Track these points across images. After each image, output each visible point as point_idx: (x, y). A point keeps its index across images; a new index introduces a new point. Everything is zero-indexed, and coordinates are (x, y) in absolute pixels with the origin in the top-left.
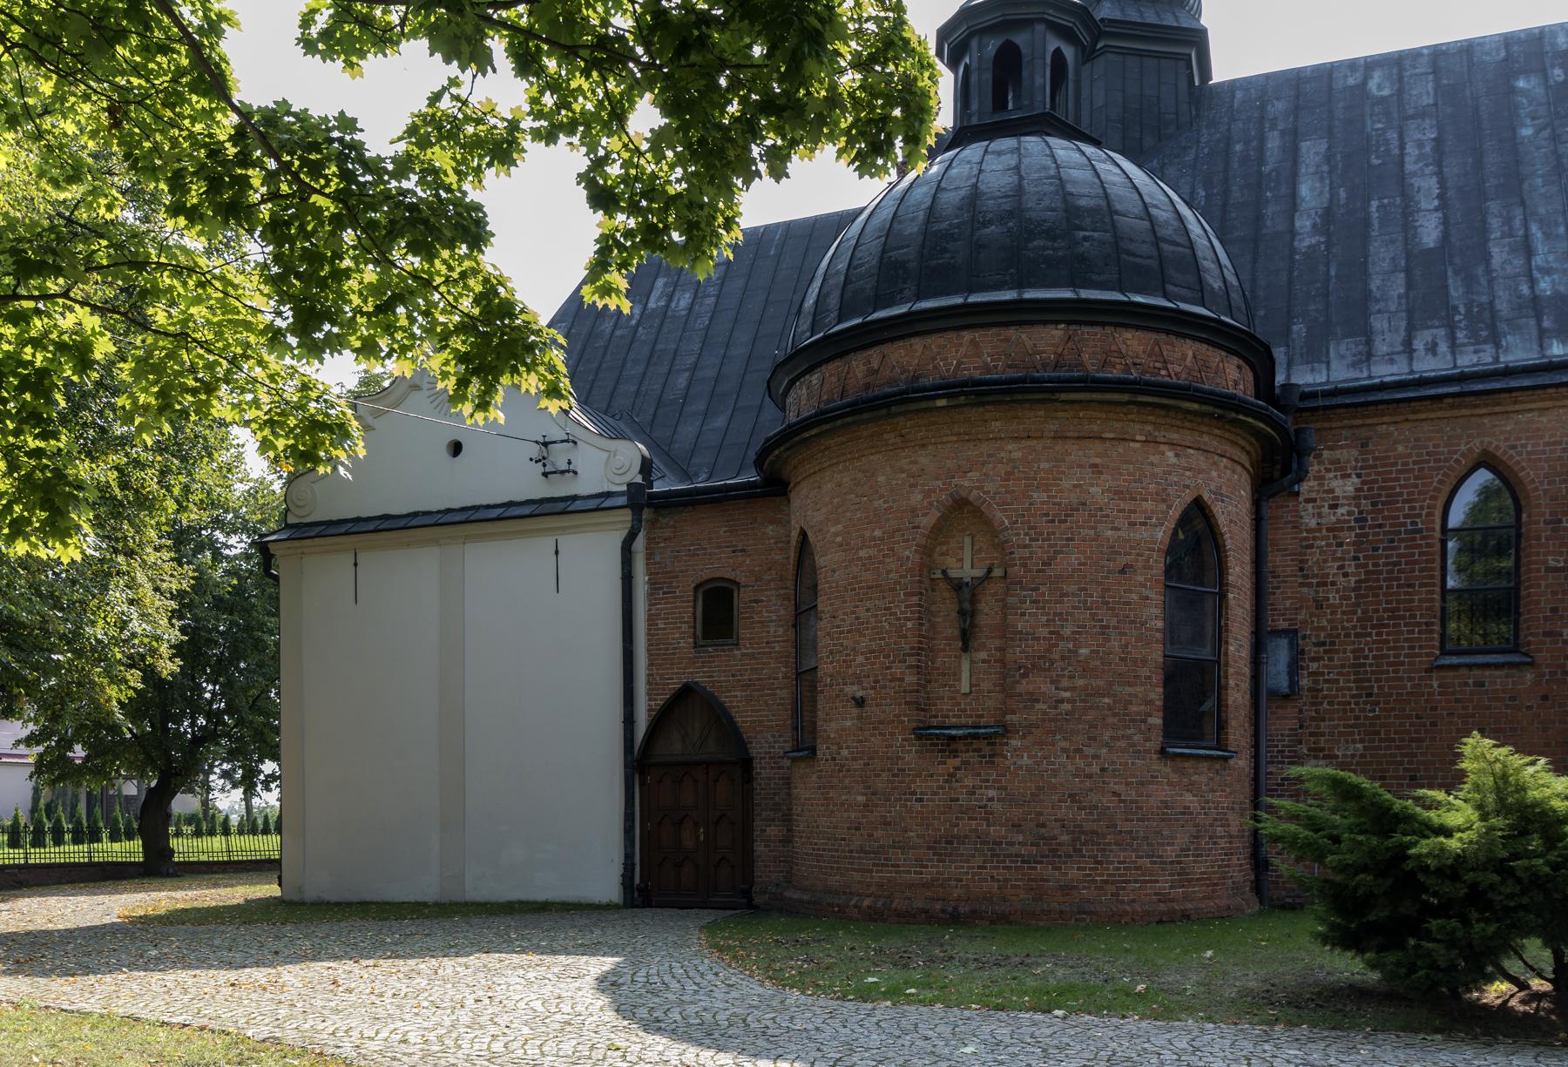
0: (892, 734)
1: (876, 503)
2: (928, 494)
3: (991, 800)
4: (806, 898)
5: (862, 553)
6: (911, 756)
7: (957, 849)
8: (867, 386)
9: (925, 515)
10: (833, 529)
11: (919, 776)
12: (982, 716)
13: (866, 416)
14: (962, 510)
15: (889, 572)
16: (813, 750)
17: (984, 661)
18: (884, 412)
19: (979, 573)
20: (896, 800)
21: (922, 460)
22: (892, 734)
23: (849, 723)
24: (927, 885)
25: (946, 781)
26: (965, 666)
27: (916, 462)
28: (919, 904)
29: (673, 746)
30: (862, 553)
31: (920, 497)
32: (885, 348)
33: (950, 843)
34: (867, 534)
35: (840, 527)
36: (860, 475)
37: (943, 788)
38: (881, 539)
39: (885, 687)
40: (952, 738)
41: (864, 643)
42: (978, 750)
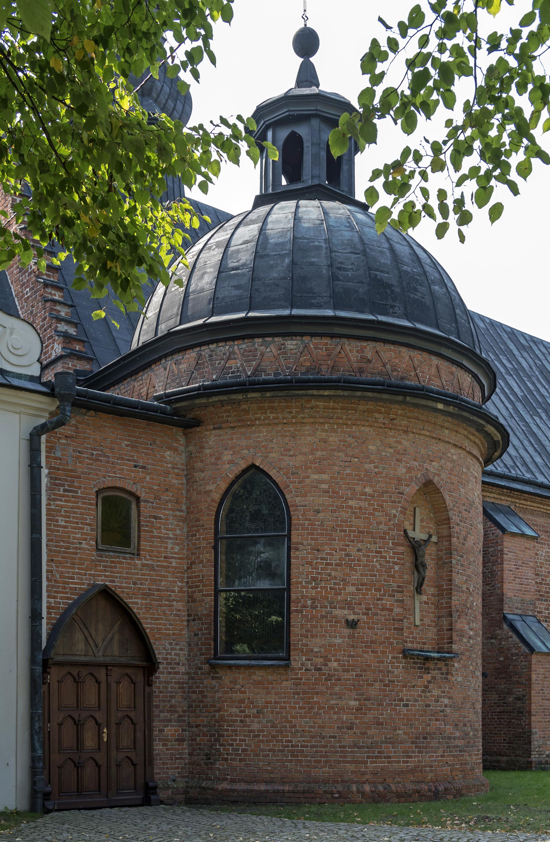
0: (383, 652)
1: (367, 466)
2: (410, 469)
4: (286, 788)
5: (351, 503)
6: (399, 670)
7: (429, 743)
8: (361, 371)
9: (407, 485)
10: (316, 477)
11: (405, 686)
12: (424, 643)
13: (385, 396)
14: (429, 488)
15: (379, 523)
16: (289, 659)
17: (426, 603)
18: (400, 398)
19: (424, 537)
20: (388, 705)
21: (405, 443)
22: (383, 652)
23: (338, 641)
24: (413, 771)
25: (423, 691)
26: (417, 605)
27: (400, 443)
28: (411, 787)
29: (78, 647)
30: (351, 503)
31: (404, 470)
32: (379, 346)
34: (358, 488)
35: (325, 477)
36: (350, 440)
37: (421, 696)
38: (372, 496)
39: (376, 614)
40: (427, 659)
41: (355, 577)
42: (440, 669)
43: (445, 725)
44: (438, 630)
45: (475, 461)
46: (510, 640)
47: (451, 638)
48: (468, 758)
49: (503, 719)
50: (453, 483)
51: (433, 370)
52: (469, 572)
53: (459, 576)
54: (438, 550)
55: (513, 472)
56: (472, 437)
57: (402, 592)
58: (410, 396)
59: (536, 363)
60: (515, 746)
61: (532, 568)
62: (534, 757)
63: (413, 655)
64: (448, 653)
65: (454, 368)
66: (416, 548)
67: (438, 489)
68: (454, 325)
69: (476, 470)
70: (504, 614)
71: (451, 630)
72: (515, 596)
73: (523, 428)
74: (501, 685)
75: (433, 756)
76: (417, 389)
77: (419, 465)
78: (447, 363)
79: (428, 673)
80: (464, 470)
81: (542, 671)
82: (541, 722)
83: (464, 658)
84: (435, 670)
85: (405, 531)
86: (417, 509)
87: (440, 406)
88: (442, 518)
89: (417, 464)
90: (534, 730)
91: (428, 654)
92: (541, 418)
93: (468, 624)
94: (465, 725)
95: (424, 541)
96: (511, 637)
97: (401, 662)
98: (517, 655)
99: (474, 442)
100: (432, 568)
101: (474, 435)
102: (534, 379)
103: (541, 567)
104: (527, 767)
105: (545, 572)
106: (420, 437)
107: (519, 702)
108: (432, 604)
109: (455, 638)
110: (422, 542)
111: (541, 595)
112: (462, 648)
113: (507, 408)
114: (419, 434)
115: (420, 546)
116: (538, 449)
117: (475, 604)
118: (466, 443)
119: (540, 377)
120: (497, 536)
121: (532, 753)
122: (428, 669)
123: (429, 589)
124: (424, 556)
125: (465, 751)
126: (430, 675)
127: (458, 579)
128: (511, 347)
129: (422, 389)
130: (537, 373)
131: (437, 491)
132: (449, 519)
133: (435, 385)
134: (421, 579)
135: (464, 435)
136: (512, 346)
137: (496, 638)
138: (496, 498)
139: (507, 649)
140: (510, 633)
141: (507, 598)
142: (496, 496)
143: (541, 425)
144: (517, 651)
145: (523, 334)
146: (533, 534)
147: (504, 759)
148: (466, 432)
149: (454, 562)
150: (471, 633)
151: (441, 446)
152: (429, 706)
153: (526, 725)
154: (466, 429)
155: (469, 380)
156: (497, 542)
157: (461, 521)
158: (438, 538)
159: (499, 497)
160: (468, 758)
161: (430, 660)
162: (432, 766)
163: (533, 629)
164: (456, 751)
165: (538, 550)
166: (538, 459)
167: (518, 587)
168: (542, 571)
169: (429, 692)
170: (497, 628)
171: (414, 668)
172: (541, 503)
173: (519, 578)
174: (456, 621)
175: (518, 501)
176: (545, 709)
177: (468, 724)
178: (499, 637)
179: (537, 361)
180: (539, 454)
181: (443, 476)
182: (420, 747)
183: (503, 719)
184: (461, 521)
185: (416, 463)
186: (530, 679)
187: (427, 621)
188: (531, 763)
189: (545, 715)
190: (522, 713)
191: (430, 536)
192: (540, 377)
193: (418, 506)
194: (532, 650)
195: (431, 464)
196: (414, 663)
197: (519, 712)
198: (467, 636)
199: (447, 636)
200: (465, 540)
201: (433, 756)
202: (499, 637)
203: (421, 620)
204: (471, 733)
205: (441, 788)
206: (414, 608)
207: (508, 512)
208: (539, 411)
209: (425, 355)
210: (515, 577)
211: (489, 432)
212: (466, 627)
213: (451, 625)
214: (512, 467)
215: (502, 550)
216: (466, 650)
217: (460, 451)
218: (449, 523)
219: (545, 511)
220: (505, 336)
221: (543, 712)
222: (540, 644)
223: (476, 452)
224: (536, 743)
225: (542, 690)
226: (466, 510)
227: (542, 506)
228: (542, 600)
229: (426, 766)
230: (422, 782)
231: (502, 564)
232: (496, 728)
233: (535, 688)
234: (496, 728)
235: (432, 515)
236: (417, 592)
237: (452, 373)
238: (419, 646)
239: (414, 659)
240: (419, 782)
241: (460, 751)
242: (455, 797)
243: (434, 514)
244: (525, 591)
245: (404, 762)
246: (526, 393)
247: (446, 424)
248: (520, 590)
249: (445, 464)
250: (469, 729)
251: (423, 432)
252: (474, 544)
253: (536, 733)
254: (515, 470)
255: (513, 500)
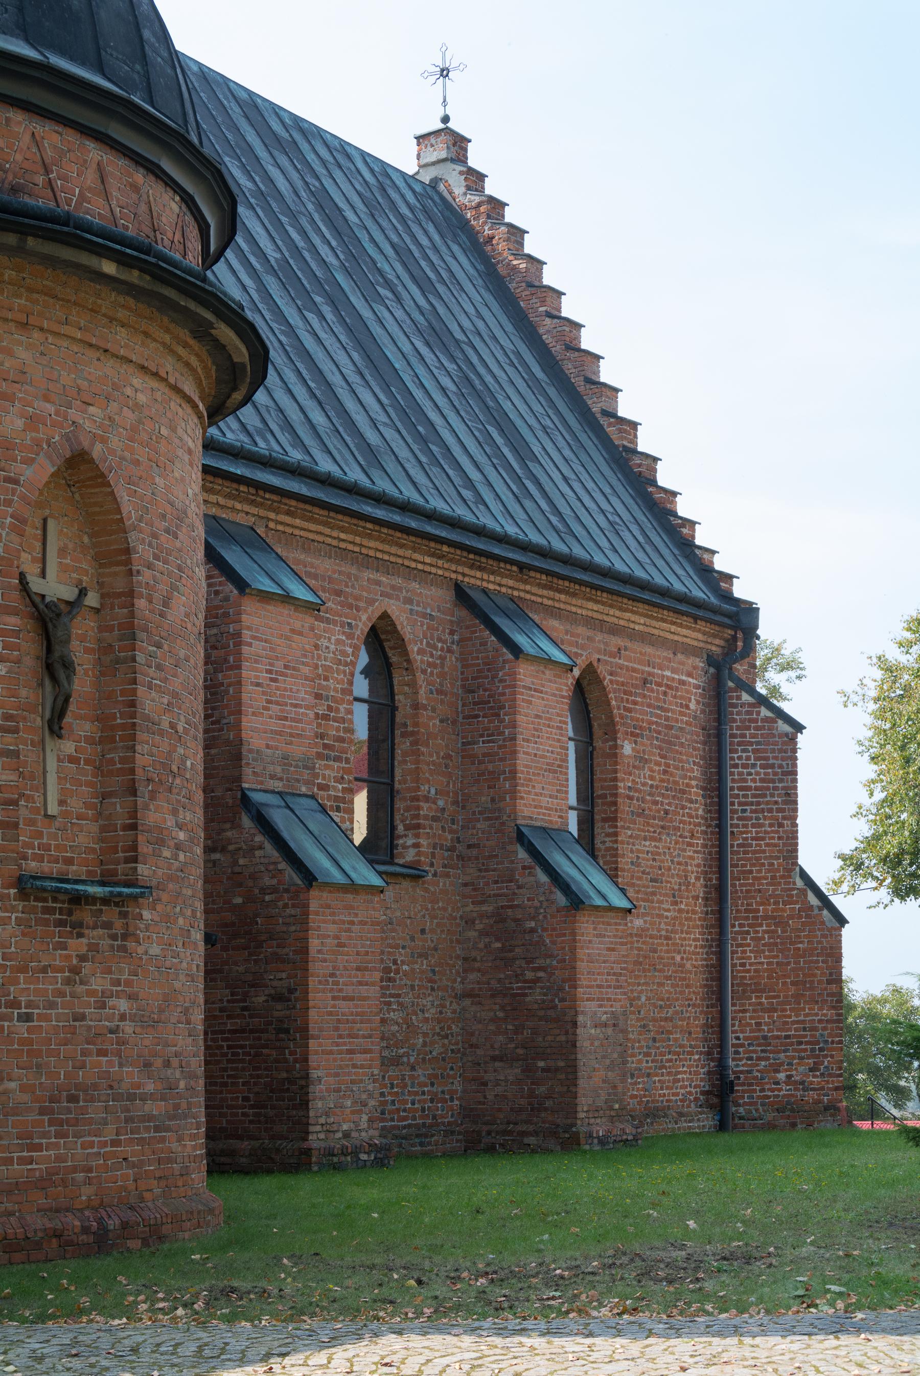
3: (123, 1017)
11: (23, 969)
12: (69, 861)
14: (80, 473)
17: (72, 760)
19: (68, 593)
24: (43, 1183)
25: (68, 982)
26: (52, 764)
28: (38, 1222)
33: (73, 1099)
37: (62, 994)
40: (77, 899)
42: (108, 925)
43: (121, 1065)
44: (103, 829)
45: (189, 410)
46: (257, 853)
47: (134, 848)
48: (174, 1145)
49: (242, 1047)
50: (137, 463)
51: (90, 177)
52: (176, 684)
53: (154, 694)
54: (101, 629)
55: (261, 444)
56: (180, 350)
57: (16, 731)
58: (36, 236)
59: (306, 183)
60: (271, 1113)
61: (306, 678)
62: (316, 1139)
63: (44, 890)
64: (127, 885)
65: (139, 176)
66: (47, 620)
67: (103, 476)
68: (138, 67)
69: (188, 433)
70: (242, 790)
71: (134, 827)
72: (268, 746)
73: (282, 338)
74: (236, 964)
75: (91, 1145)
76: (53, 218)
77: (57, 413)
78: (122, 162)
79: (80, 935)
80: (164, 431)
81: (332, 929)
82: (331, 1052)
83: (165, 897)
84: (95, 927)
85: (22, 577)
86: (51, 524)
87: (109, 268)
88: (112, 551)
89: (51, 408)
90: (314, 1074)
91: (80, 887)
92: (322, 317)
93: (175, 812)
94: (167, 1064)
95: (68, 603)
96: (261, 848)
97: (13, 909)
98: (274, 890)
99: (187, 364)
100: (86, 671)
101: (186, 345)
102: (304, 221)
103: (326, 679)
104: (299, 1162)
105: (336, 690)
106: (59, 342)
107: (279, 1006)
108: (87, 762)
109: (144, 848)
110: (62, 606)
111: (325, 746)
112: (160, 872)
113: (244, 287)
114: (57, 334)
115: (59, 615)
116: (318, 393)
117: (189, 763)
118: (168, 366)
119: (316, 217)
120: (227, 599)
121: (311, 1129)
122: (81, 925)
123: (80, 725)
124: (68, 641)
125: (168, 1129)
126: (84, 941)
127: (150, 702)
128: (249, 139)
129: (66, 220)
130: (310, 207)
131: (100, 479)
132: (127, 551)
133: (95, 211)
134: (60, 702)
135: (164, 344)
136: (251, 137)
137: (223, 850)
138: (222, 507)
139: (253, 876)
140: (259, 838)
141: (250, 751)
142: (222, 501)
143: (322, 335)
144: (275, 881)
145: (276, 110)
146: (310, 597)
147: (245, 1145)
148: (167, 338)
149: (140, 658)
150: (182, 835)
151: (109, 368)
152: (83, 1017)
153: (296, 1061)
154: (167, 331)
155: (175, 207)
156: (226, 615)
157: (156, 557)
158: (103, 596)
159: (230, 503)
160: (174, 1145)
161: (84, 902)
162: (90, 1170)
163: (312, 826)
164: (147, 1129)
165: (319, 637)
166: (318, 417)
167: (275, 724)
168: (327, 688)
169: (82, 983)
170: (228, 826)
171: (46, 923)
172: (326, 524)
173: (277, 703)
174: (146, 807)
175: (272, 515)
176: (339, 1021)
177: (175, 1062)
178: (231, 848)
179: (309, 179)
180: (320, 403)
181: (115, 442)
182: (61, 1123)
183: (242, 1047)
184: (156, 557)
185: (48, 405)
186: (305, 950)
187: (75, 805)
188: (308, 1152)
189: (340, 1037)
190: (287, 1031)
191: (83, 593)
192: (316, 217)
193: (52, 516)
194: (309, 877)
195: (84, 412)
196: (46, 910)
197: (279, 1031)
198: (172, 843)
199: (124, 841)
200: (166, 604)
201: (91, 1145)
202: (231, 848)
203: (61, 803)
204: (182, 1084)
205: (113, 1223)
206: (45, 772)
207: (253, 542)
208: (318, 299)
209: (71, 137)
210: (269, 702)
211: (223, 341)
212: (170, 822)
213: (134, 814)
214: (260, 433)
215: (238, 634)
216: (171, 878)
217: (155, 384)
218: (129, 562)
219: (335, 543)
220: (235, 111)
221: (337, 1029)
222: (326, 864)
223: (189, 388)
224: (320, 1104)
225: (332, 975)
226: (167, 531)
227: (327, 531)
228: (328, 758)
229: (75, 1169)
230: (67, 1210)
231: (239, 667)
232: (225, 1070)
233: (318, 969)
234: (225, 1070)
235: (86, 539)
236: (52, 731)
237: (135, 188)
238: (55, 869)
239: (45, 900)
240: (57, 1211)
241: (157, 1129)
242: (145, 1243)
243: (91, 537)
244: (291, 735)
245: (22, 1161)
246: (287, 254)
247: (121, 314)
248: (280, 733)
249: (120, 413)
250: (178, 1074)
251: (64, 329)
252: (187, 615)
253: (319, 1080)
254: (266, 440)
255: (262, 513)
